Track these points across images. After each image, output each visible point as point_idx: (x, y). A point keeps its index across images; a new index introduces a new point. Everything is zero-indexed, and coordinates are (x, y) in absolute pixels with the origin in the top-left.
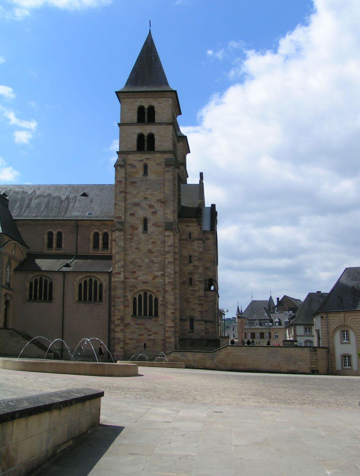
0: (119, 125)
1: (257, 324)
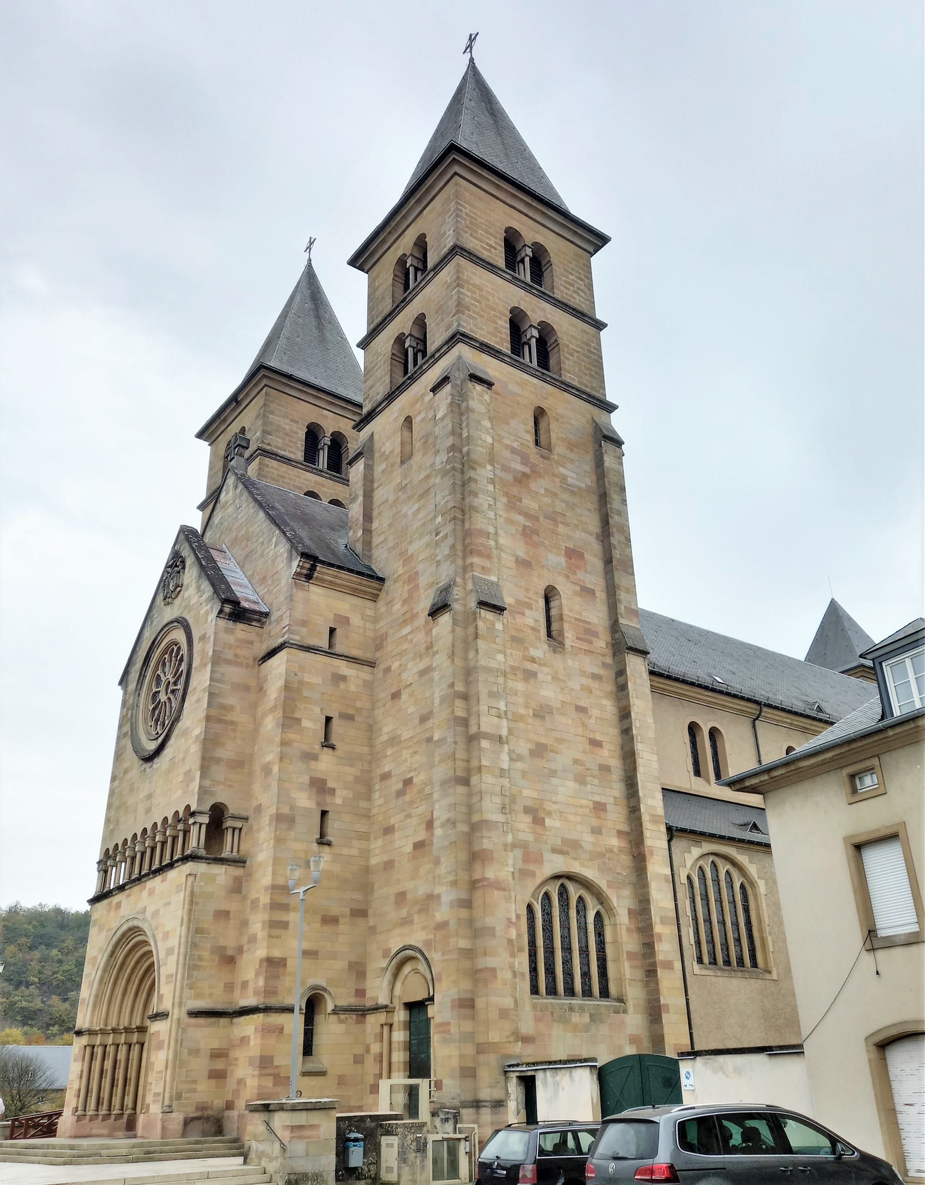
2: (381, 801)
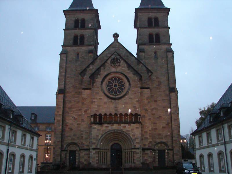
1: (129, 162)
2: (153, 118)
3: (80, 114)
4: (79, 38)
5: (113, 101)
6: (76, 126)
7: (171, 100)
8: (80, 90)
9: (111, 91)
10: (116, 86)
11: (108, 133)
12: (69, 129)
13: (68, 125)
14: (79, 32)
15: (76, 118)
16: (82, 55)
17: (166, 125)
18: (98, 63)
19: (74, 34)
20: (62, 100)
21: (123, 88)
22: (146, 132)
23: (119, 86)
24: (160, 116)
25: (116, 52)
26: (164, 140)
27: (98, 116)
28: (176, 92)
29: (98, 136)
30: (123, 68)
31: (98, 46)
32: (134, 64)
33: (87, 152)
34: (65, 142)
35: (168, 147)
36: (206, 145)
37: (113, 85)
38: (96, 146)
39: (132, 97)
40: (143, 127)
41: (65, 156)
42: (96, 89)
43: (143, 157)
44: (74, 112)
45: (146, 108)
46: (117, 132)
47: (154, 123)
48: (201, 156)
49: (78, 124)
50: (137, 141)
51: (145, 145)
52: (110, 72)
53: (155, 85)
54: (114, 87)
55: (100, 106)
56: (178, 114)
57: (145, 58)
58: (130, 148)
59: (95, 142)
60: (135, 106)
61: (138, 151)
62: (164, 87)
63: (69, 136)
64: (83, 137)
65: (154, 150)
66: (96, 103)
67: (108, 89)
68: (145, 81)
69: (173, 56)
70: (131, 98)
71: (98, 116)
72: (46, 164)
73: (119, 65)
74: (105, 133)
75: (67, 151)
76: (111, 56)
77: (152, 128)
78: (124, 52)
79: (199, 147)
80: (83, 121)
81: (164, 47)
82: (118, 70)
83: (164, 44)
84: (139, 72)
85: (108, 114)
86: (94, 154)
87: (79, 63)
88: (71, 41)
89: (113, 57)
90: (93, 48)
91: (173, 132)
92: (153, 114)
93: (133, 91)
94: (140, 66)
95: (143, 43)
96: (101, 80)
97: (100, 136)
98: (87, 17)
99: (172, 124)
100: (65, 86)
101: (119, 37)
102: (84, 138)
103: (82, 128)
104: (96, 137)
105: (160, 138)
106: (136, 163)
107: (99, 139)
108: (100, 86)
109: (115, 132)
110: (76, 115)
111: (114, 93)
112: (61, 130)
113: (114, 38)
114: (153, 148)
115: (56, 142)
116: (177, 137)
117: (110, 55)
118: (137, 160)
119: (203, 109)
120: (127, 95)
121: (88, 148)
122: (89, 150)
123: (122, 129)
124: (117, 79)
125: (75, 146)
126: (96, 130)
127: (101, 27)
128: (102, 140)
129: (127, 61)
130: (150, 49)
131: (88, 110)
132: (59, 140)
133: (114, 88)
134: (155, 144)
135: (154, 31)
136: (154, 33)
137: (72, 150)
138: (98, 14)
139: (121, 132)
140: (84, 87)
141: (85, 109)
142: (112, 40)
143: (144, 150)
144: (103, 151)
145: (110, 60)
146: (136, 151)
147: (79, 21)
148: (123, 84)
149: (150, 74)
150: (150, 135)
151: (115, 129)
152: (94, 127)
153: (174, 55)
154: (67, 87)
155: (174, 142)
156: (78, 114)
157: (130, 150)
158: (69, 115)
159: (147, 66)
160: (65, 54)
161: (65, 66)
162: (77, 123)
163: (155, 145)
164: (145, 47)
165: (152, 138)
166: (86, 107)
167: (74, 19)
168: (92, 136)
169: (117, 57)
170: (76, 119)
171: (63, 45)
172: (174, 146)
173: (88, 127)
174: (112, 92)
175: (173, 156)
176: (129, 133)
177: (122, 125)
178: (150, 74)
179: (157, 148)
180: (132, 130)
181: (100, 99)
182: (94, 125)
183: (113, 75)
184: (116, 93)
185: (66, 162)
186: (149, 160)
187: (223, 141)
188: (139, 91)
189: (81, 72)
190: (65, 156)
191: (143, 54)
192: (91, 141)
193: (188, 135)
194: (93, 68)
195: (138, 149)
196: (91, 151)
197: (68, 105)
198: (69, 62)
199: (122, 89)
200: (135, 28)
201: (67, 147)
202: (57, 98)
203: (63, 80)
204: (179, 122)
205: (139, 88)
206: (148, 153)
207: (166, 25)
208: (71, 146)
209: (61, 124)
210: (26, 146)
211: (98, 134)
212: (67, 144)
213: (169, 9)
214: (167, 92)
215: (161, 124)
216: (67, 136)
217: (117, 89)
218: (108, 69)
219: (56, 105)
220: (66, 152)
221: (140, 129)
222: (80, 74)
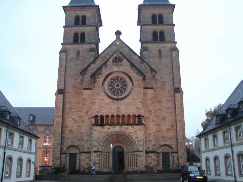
0: (64, 27)
1: (131, 165)
3: (80, 115)
4: (79, 35)
5: (115, 101)
6: (76, 127)
7: (176, 101)
8: (80, 90)
9: (113, 91)
10: (118, 85)
11: (109, 135)
12: (69, 131)
13: (68, 127)
14: (79, 29)
15: (76, 119)
16: (83, 54)
17: (171, 126)
18: (99, 62)
19: (74, 32)
20: (62, 101)
21: (126, 88)
22: (150, 134)
23: (121, 86)
24: (165, 117)
25: (118, 50)
26: (168, 143)
27: (99, 117)
28: (181, 93)
29: (99, 138)
30: (125, 68)
31: (100, 44)
32: (137, 62)
33: (88, 155)
34: (65, 144)
35: (173, 150)
36: (212, 148)
37: (115, 85)
38: (98, 149)
39: (135, 97)
40: (146, 129)
41: (64, 159)
42: (98, 89)
43: (146, 160)
44: (74, 113)
45: (149, 109)
46: (119, 134)
47: (158, 125)
48: (207, 160)
49: (78, 126)
50: (141, 143)
51: (148, 148)
52: (113, 71)
53: (159, 85)
54: (116, 87)
55: (101, 107)
56: (183, 115)
57: (149, 57)
58: (133, 151)
59: (96, 144)
60: (138, 107)
61: (141, 154)
62: (169, 87)
63: (69, 139)
64: (83, 139)
65: (158, 153)
66: (97, 104)
67: (110, 90)
68: (149, 81)
69: (178, 55)
70: (134, 99)
71: (99, 117)
72: (45, 168)
73: (122, 64)
74: (107, 135)
75: (67, 154)
76: (113, 55)
77: (156, 131)
78: (127, 50)
79: (204, 150)
80: (84, 123)
81: (169, 45)
82: (121, 69)
83: (170, 42)
84: (142, 71)
85: (110, 115)
86: (95, 156)
87: (80, 62)
88: (71, 39)
89: (115, 55)
90: (94, 46)
91: (178, 134)
92: (156, 116)
93: (136, 91)
94: (144, 66)
95: (147, 41)
96: (103, 80)
97: (102, 138)
98: (88, 13)
99: (177, 126)
100: (65, 86)
101: (121, 34)
102: (84, 140)
103: (83, 130)
104: (97, 139)
105: (164, 141)
106: (139, 166)
107: (100, 142)
108: (101, 86)
109: (117, 134)
110: (76, 117)
111: (116, 93)
112: (61, 133)
113: (116, 36)
114: (157, 151)
115: (56, 145)
116: (182, 140)
117: (113, 54)
118: (141, 163)
119: (209, 110)
120: (129, 95)
121: (89, 151)
122: (90, 152)
123: (124, 131)
124: (120, 79)
125: (75, 148)
126: (98, 132)
127: (103, 24)
128: (104, 142)
129: (129, 59)
130: (154, 47)
131: (89, 111)
132: (58, 143)
133: (116, 88)
134: (159, 146)
135: (158, 28)
136: (158, 31)
137: (72, 153)
138: (99, 10)
139: (123, 134)
140: (85, 87)
141: (85, 110)
142: (114, 38)
143: (147, 152)
144: (105, 154)
145: (112, 58)
146: (139, 154)
147: (79, 18)
148: (126, 83)
149: (154, 74)
150: (154, 137)
151: (117, 131)
152: (95, 129)
153: (179, 53)
154: (67, 87)
155: (179, 144)
156: (78, 115)
157: (133, 153)
158: (70, 116)
159: (151, 66)
160: (65, 52)
161: (64, 65)
162: (78, 124)
163: (159, 148)
164: (149, 45)
165: (156, 141)
166: (87, 108)
167: (74, 16)
168: (93, 138)
169: (120, 55)
170: (77, 120)
171: (62, 43)
172: (179, 148)
173: (89, 129)
174: (114, 92)
175: (178, 158)
176: (132, 136)
177: (125, 127)
178: (154, 74)
179: (160, 150)
180: (135, 132)
181: (102, 99)
182: (95, 126)
183: (115, 75)
184: (118, 93)
185: (66, 166)
186: (153, 163)
187: (230, 144)
188: (143, 92)
189: (82, 72)
190: (64, 159)
191: (147, 52)
192: (92, 143)
193: (193, 137)
194: (94, 67)
195: (142, 151)
196: (92, 154)
197: (68, 106)
198: (70, 61)
199: (125, 89)
200: (138, 25)
201: (67, 150)
202: (57, 99)
203: (63, 79)
204: (184, 124)
205: (142, 88)
206: (151, 157)
207: (171, 22)
208: (71, 148)
209: (61, 126)
210: (24, 149)
211: (99, 136)
212: (67, 147)
213: (174, 5)
214: (172, 92)
215: (165, 126)
216: (67, 139)
217: (119, 90)
218: (110, 68)
219: (56, 105)
220: (66, 155)
221: (143, 131)
222: (80, 74)
